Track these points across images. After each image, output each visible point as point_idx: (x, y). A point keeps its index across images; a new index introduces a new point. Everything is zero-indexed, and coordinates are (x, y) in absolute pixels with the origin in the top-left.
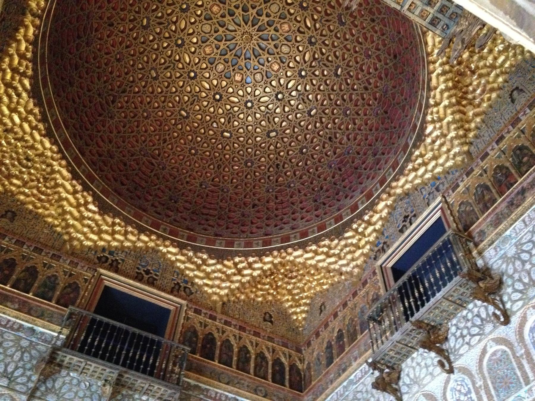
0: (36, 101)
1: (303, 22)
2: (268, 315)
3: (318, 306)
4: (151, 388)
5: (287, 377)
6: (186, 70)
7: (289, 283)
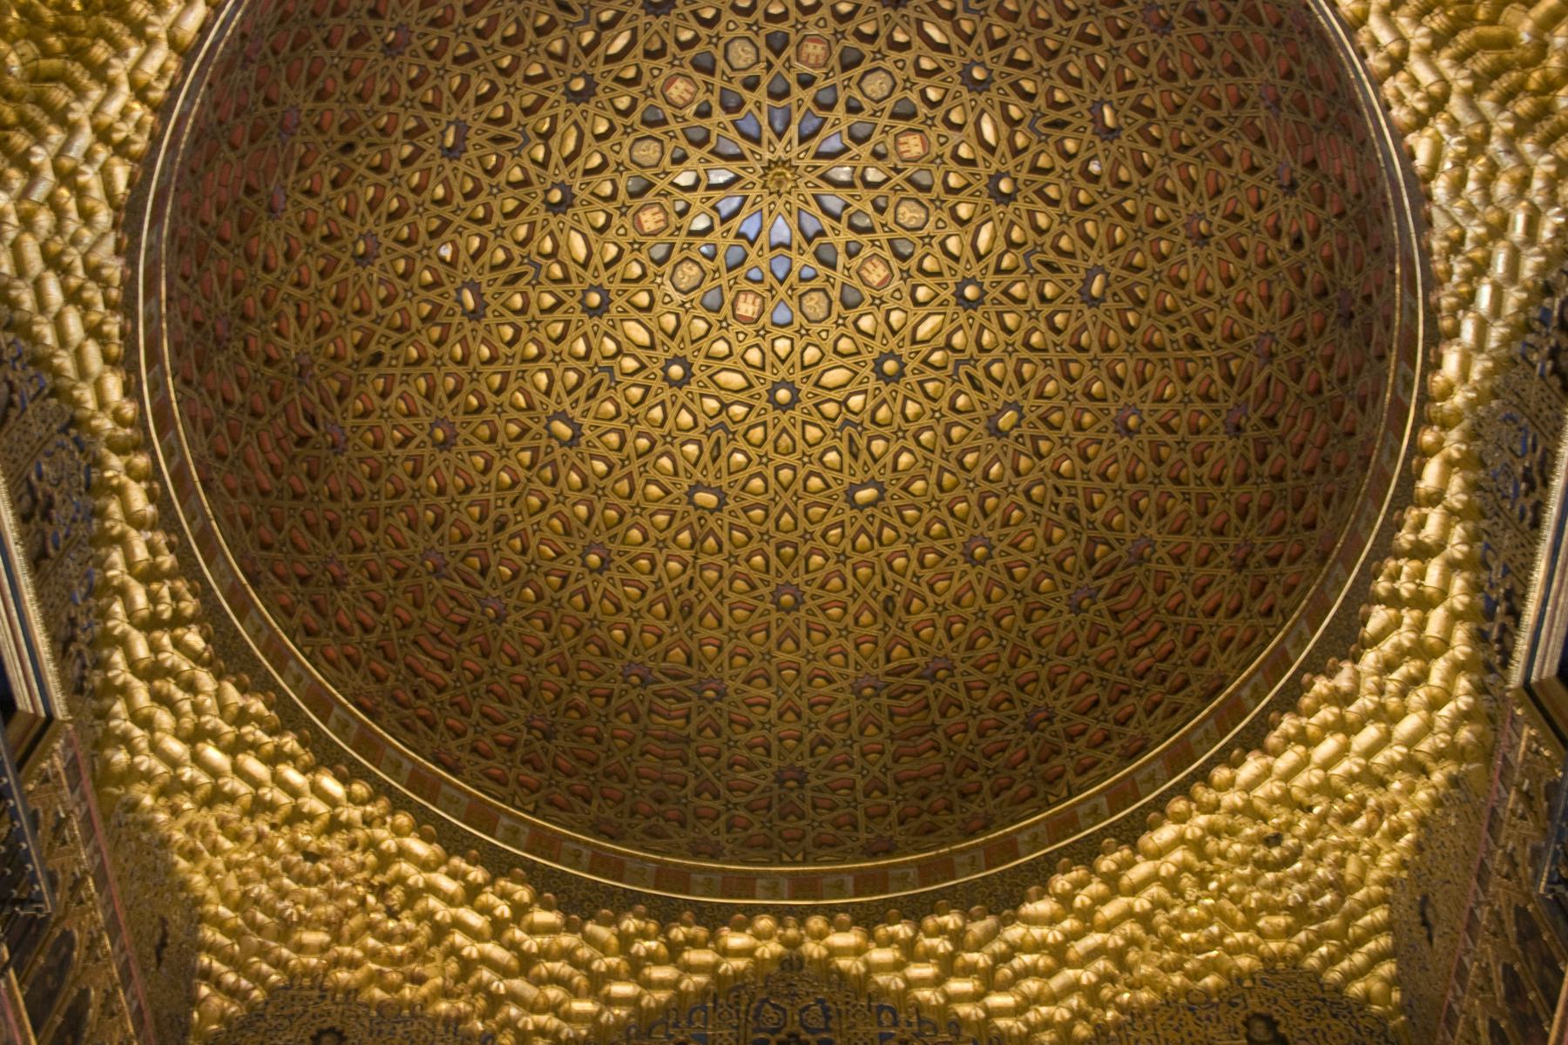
0: (1033, 890)
1: (628, 60)
6: (962, 319)
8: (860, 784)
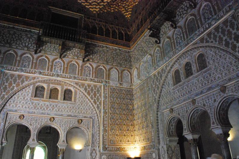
2: (116, 17)
3: (135, 11)
4: (75, 45)
5: (124, 38)
7: (123, 4)
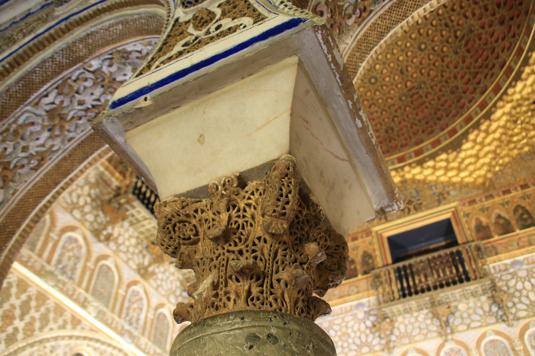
0: (464, 141)
8: (409, 125)
